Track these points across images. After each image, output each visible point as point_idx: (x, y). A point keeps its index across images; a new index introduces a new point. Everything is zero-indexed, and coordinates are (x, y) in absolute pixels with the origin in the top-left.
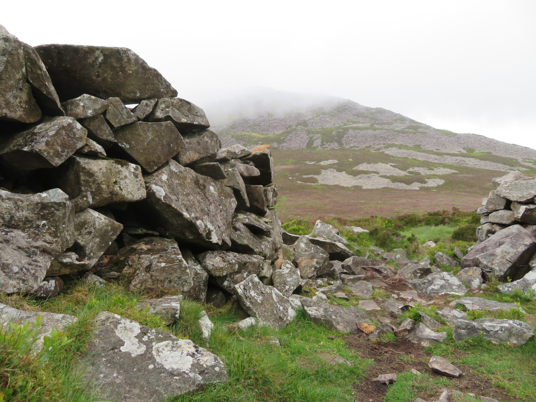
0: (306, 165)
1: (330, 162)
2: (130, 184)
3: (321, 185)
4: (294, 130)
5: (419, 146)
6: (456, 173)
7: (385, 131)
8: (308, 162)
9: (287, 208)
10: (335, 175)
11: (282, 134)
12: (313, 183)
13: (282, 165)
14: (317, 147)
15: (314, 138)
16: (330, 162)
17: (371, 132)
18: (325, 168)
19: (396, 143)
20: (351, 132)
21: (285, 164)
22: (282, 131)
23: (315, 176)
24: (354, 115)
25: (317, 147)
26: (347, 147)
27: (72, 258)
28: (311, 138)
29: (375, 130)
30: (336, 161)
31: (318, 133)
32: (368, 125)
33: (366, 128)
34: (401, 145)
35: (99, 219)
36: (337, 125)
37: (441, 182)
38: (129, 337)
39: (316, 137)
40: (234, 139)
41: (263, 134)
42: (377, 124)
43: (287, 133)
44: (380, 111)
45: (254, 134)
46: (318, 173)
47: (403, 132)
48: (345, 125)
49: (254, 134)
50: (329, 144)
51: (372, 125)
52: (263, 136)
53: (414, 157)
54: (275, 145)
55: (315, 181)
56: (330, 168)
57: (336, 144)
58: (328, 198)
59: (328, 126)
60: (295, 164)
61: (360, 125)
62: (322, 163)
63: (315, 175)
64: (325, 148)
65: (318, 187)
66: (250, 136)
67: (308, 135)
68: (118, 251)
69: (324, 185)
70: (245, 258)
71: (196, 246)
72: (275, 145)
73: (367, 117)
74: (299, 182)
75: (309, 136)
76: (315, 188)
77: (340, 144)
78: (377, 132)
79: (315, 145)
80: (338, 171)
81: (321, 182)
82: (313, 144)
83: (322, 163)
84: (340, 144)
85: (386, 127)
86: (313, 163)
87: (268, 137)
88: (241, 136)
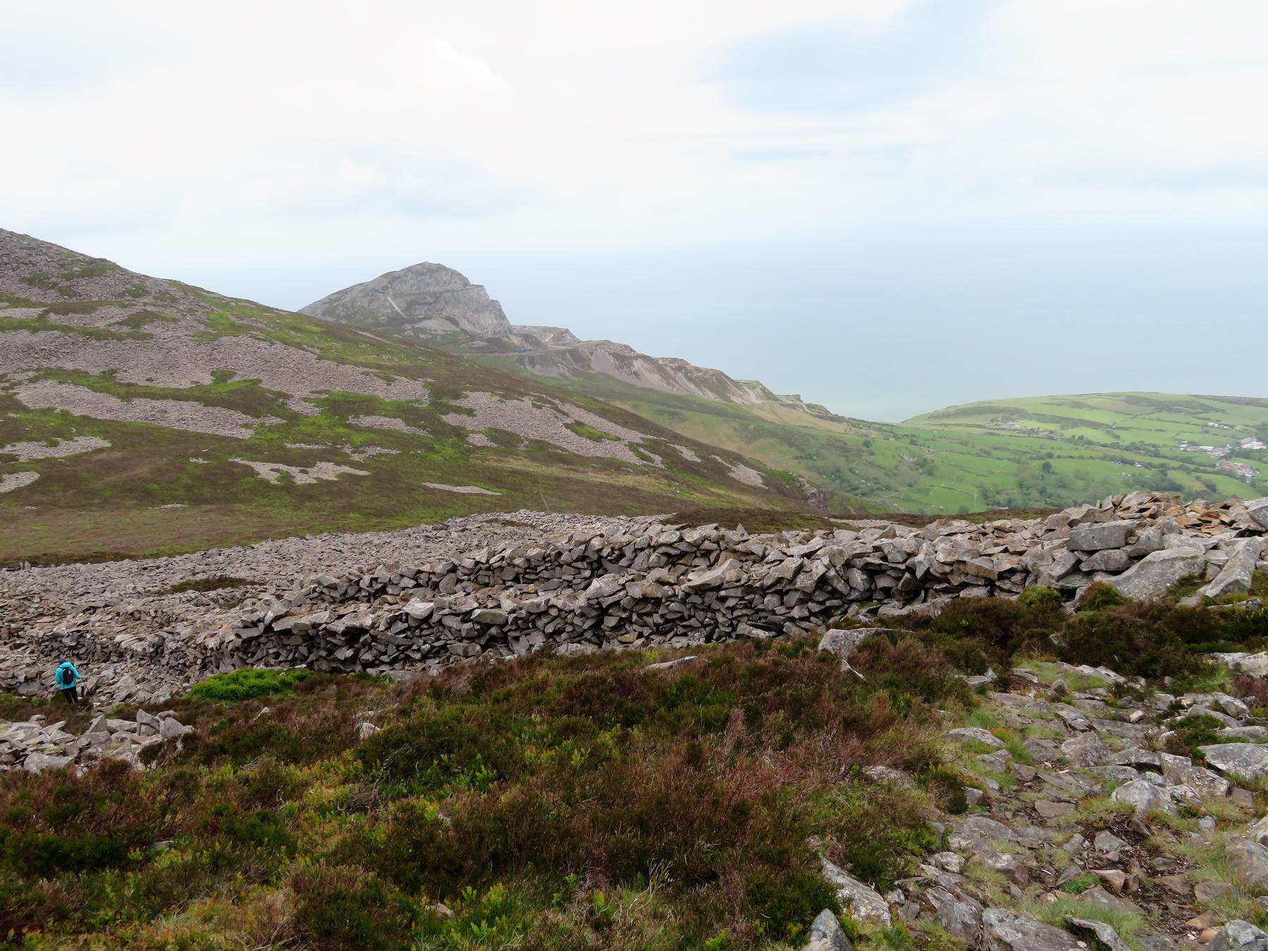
5: (114, 372)
6: (101, 450)
7: (57, 333)
17: (24, 336)
19: (69, 366)
24: (22, 281)
29: (35, 331)
33: (19, 326)
34: (76, 371)
37: (28, 478)
42: (56, 312)
44: (97, 268)
47: (98, 335)
53: (67, 408)
61: (19, 313)
73: (55, 284)
78: (42, 334)
85: (75, 320)
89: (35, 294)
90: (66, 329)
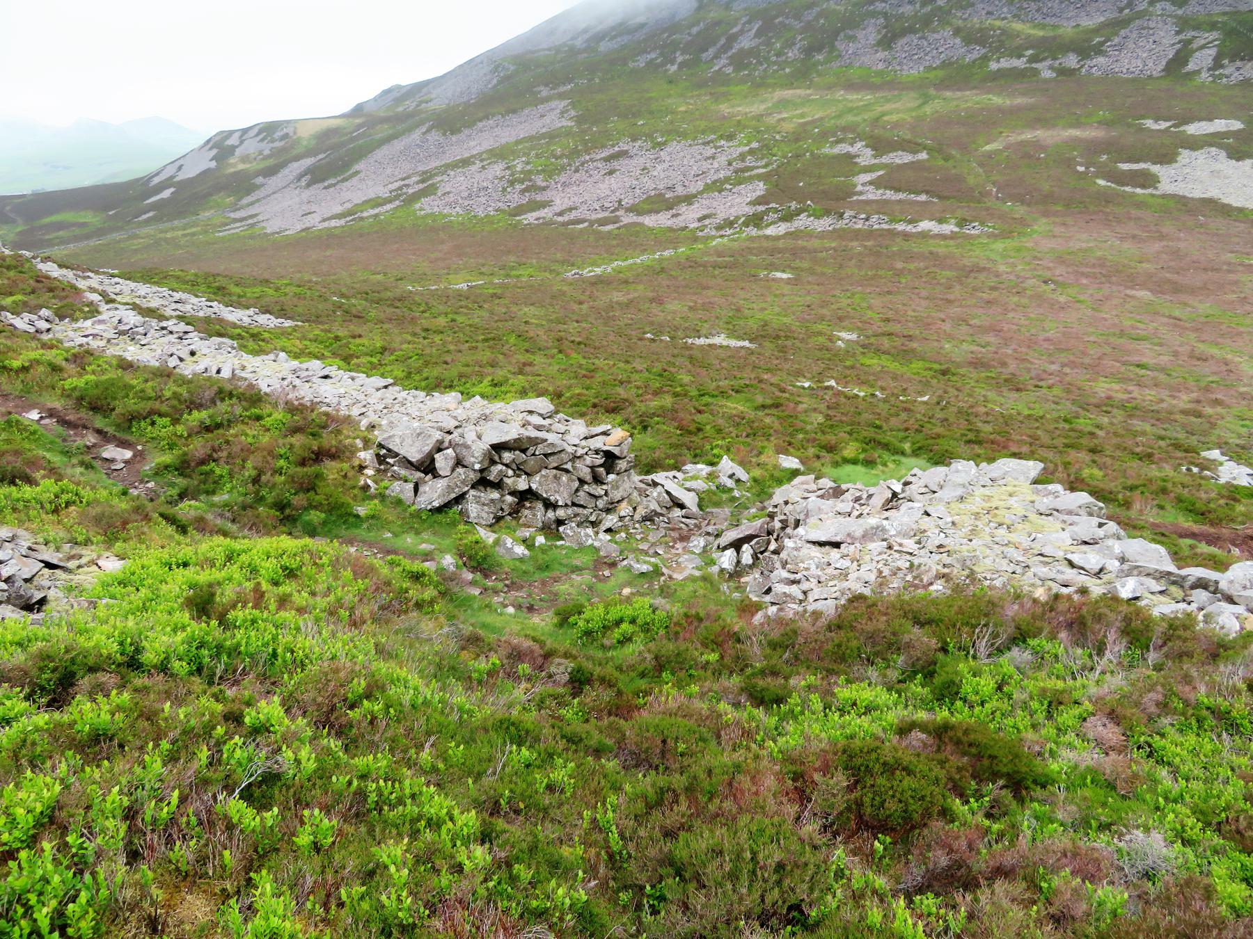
0: (1141, 129)
1: (1219, 125)
2: (522, 484)
3: (1164, 196)
8: (1149, 124)
9: (1035, 258)
10: (1218, 166)
11: (1103, 26)
12: (1143, 187)
13: (1071, 126)
14: (1198, 72)
15: (1195, 46)
16: (1219, 125)
18: (1195, 144)
21: (1078, 125)
22: (1102, 19)
23: (1155, 169)
25: (1198, 72)
27: (500, 513)
28: (1187, 43)
30: (1237, 125)
31: (1213, 26)
35: (509, 499)
38: (509, 542)
39: (1203, 42)
40: (958, 41)
41: (1043, 27)
45: (1017, 26)
46: (1167, 158)
49: (1017, 26)
50: (1238, 63)
52: (1041, 33)
54: (1071, 61)
55: (1148, 180)
56: (1211, 145)
58: (1162, 237)
60: (1106, 124)
62: (1193, 129)
63: (1155, 163)
64: (1221, 76)
65: (1151, 200)
66: (1004, 31)
67: (1178, 33)
68: (515, 512)
69: (1173, 196)
70: (580, 510)
71: (549, 505)
72: (1071, 61)
74: (1101, 182)
75: (1182, 37)
76: (1140, 205)
79: (1191, 66)
80: (1230, 157)
81: (1166, 187)
82: (1186, 63)
83: (1193, 129)
86: (1163, 125)
87: (1054, 38)
88: (981, 30)
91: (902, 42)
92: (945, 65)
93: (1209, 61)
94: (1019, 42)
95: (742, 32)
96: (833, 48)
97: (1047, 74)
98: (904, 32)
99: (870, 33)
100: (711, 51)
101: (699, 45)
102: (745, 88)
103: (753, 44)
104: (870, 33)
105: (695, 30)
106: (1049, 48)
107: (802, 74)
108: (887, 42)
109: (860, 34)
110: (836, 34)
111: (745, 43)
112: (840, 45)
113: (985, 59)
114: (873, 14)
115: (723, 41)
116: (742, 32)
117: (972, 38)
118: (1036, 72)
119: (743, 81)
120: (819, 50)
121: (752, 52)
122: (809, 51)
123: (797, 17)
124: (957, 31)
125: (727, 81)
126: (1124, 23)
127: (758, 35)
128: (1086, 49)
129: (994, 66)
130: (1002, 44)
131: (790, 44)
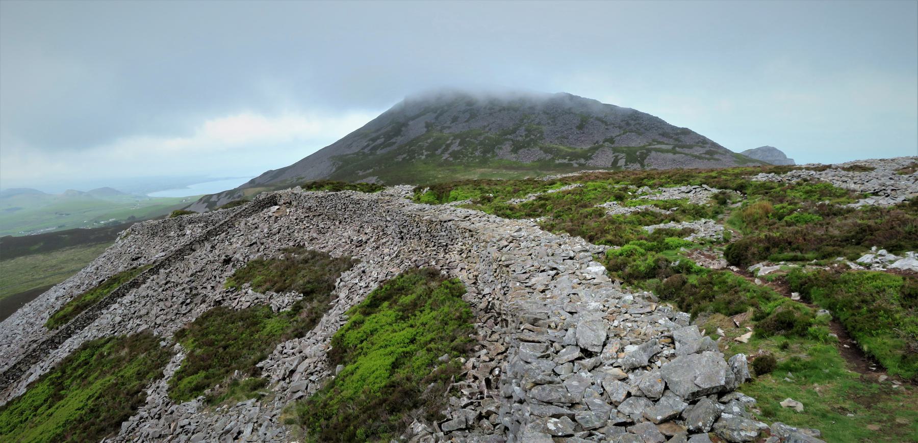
4: (601, 146)
17: (670, 156)
20: (653, 154)
26: (648, 169)
28: (616, 157)
31: (623, 152)
32: (670, 147)
33: (667, 151)
36: (642, 145)
42: (679, 147)
43: (594, 149)
44: (686, 132)
45: (561, 147)
48: (650, 144)
49: (561, 147)
51: (674, 148)
54: (582, 161)
57: (639, 165)
59: (633, 145)
61: (664, 147)
72: (582, 161)
77: (642, 165)
78: (677, 156)
79: (619, 164)
84: (642, 165)
85: (686, 151)
89: (665, 140)
90: (686, 155)
91: (521, 151)
92: (539, 160)
93: (624, 163)
94: (563, 153)
95: (452, 143)
96: (494, 152)
97: (576, 166)
98: (521, 148)
99: (507, 147)
100: (439, 151)
101: (433, 147)
102: (462, 167)
103: (459, 148)
104: (507, 147)
105: (429, 141)
106: (575, 156)
107: (484, 162)
108: (515, 150)
109: (504, 147)
110: (494, 146)
111: (455, 147)
112: (497, 151)
113: (553, 159)
114: (507, 140)
115: (444, 147)
116: (452, 143)
117: (547, 151)
118: (572, 165)
119: (460, 164)
120: (489, 152)
121: (458, 151)
122: (485, 152)
123: (476, 139)
124: (541, 148)
125: (452, 164)
126: (597, 149)
127: (460, 144)
128: (587, 158)
129: (557, 162)
130: (558, 154)
131: (475, 149)
